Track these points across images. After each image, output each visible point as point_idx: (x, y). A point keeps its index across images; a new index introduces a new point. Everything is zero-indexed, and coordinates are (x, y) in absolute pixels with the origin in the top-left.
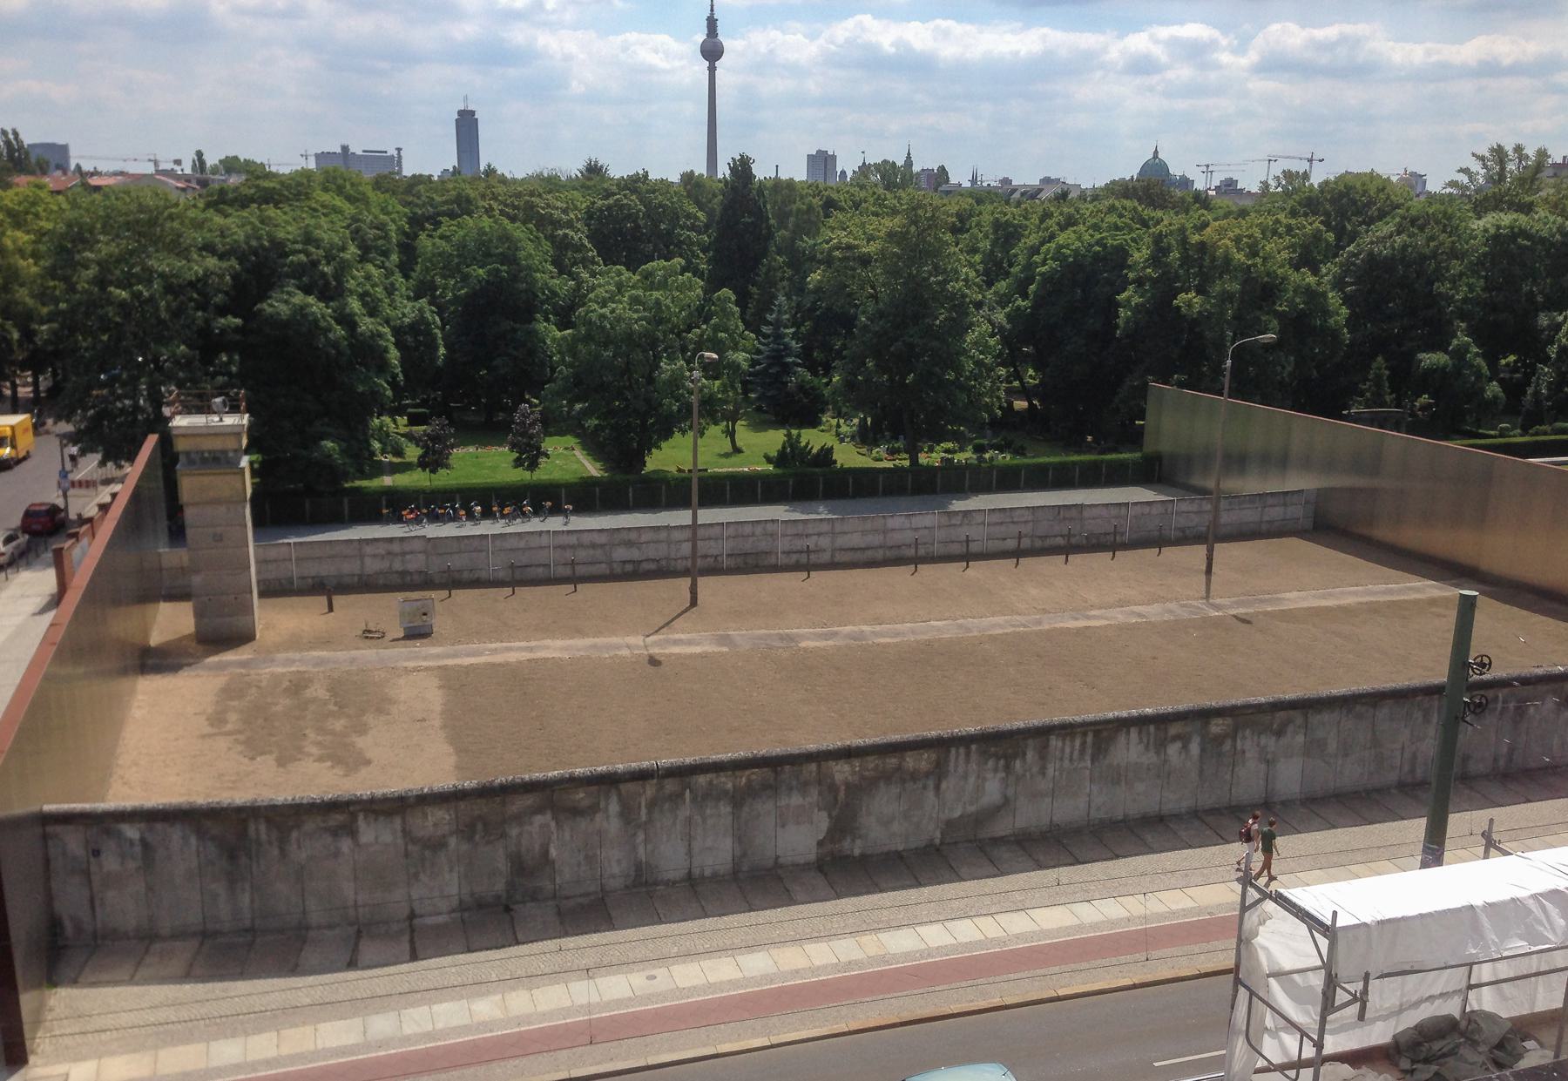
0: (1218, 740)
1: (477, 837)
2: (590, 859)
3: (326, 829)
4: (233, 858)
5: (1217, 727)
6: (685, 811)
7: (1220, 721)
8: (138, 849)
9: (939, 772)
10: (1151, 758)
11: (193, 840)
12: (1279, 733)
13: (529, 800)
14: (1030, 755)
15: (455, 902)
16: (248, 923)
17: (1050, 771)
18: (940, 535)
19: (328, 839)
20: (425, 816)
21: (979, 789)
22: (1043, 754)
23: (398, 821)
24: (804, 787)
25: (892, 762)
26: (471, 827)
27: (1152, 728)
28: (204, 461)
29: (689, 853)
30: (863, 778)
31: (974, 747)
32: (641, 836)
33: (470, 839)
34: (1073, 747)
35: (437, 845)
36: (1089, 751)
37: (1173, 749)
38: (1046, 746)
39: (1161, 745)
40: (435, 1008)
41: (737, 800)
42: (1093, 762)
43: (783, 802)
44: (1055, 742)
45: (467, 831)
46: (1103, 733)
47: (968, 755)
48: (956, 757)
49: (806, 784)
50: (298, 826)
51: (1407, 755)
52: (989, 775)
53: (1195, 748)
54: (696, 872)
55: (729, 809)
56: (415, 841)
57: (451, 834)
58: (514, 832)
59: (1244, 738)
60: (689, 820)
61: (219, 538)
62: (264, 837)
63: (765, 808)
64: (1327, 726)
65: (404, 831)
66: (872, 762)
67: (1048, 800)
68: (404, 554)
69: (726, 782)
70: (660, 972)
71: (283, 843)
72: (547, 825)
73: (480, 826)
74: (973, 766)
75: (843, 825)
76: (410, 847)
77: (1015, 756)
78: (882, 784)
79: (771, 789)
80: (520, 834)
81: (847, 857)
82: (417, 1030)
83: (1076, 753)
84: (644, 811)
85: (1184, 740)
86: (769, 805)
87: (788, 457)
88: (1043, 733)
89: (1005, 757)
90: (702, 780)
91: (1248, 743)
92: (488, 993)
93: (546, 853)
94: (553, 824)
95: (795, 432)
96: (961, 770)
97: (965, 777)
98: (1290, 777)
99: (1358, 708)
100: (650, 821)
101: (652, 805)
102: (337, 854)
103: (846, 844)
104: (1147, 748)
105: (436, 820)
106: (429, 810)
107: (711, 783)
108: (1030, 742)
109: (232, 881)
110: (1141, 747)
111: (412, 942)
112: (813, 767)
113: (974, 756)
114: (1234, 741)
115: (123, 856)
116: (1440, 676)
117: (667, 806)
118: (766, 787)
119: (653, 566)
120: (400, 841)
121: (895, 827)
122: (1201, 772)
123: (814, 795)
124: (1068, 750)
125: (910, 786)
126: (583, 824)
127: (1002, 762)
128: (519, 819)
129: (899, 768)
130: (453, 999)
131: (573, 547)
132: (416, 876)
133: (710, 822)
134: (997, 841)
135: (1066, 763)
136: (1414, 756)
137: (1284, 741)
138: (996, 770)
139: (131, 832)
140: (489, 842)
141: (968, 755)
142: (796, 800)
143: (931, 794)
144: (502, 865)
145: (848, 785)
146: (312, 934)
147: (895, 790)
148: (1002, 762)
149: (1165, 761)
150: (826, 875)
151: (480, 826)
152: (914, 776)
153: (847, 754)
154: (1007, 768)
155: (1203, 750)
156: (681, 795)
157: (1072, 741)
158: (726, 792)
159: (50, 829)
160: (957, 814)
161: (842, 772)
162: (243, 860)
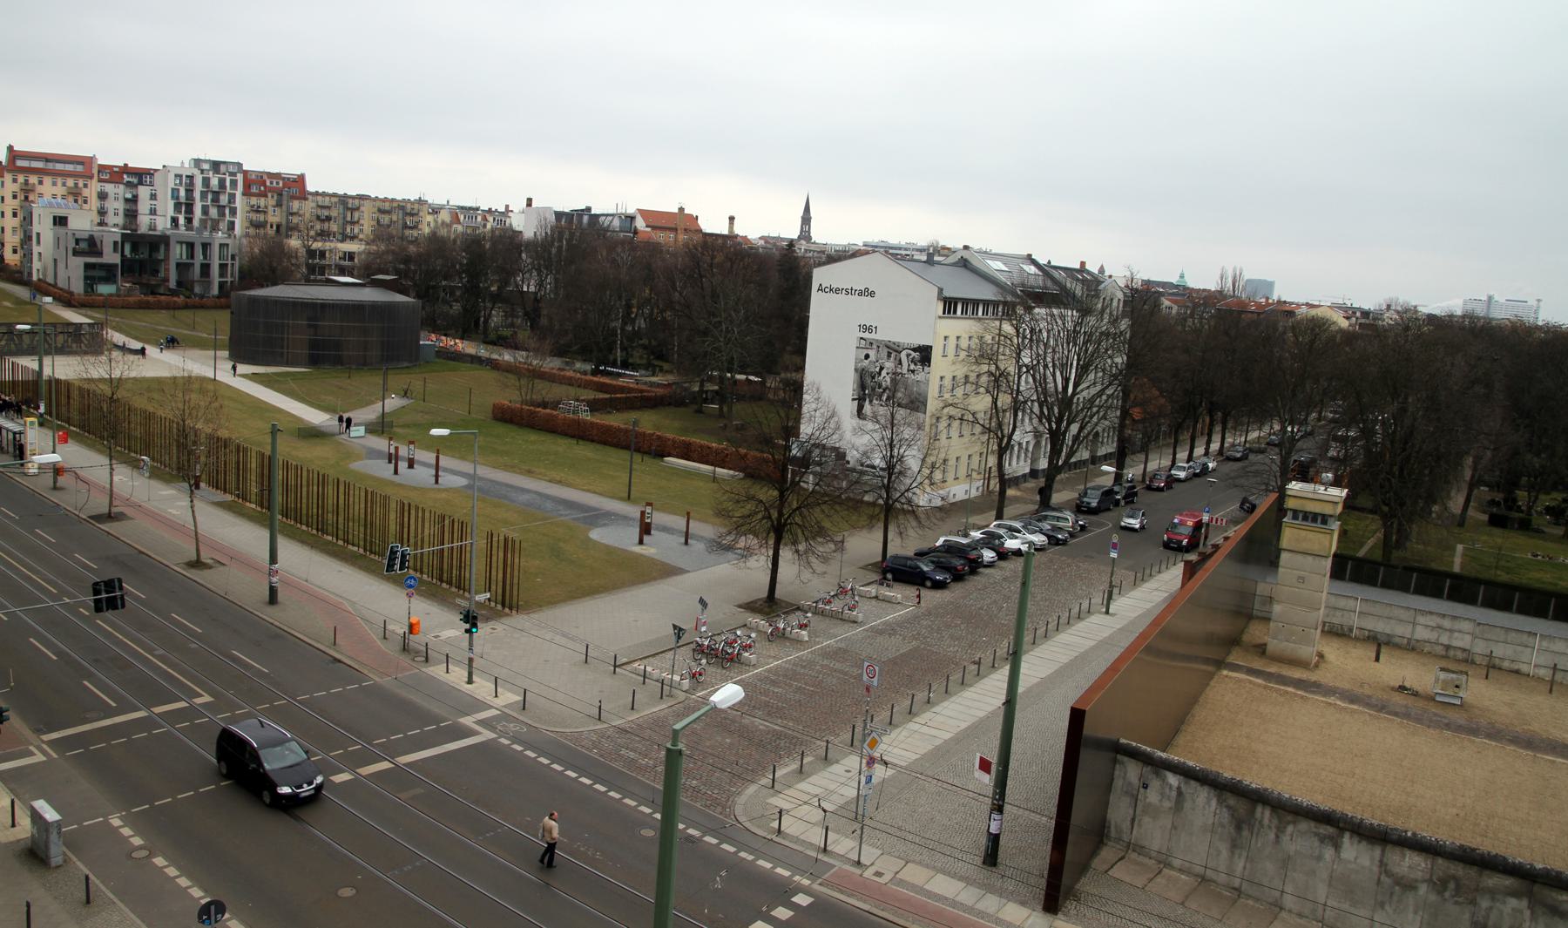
1: (1447, 894)
3: (1316, 834)
4: (1239, 828)
8: (1174, 794)
11: (1214, 803)
13: (1508, 882)
19: (1317, 843)
20: (1404, 856)
23: (1377, 851)
28: (1305, 518)
33: (1440, 893)
35: (1408, 886)
45: (1440, 885)
50: (1294, 823)
56: (1388, 874)
57: (1424, 881)
58: (1485, 903)
61: (1302, 579)
62: (1266, 822)
65: (1381, 861)
68: (1451, 631)
71: (1280, 830)
72: (1521, 912)
73: (1452, 885)
76: (1383, 878)
80: (1491, 908)
94: (1527, 913)
102: (1319, 858)
105: (1410, 864)
106: (1408, 853)
109: (1234, 846)
120: (1375, 869)
128: (1493, 893)
132: (1382, 905)
139: (1173, 780)
140: (1456, 903)
146: (1284, 914)
151: (1452, 885)
159: (1119, 757)
162: (1245, 833)
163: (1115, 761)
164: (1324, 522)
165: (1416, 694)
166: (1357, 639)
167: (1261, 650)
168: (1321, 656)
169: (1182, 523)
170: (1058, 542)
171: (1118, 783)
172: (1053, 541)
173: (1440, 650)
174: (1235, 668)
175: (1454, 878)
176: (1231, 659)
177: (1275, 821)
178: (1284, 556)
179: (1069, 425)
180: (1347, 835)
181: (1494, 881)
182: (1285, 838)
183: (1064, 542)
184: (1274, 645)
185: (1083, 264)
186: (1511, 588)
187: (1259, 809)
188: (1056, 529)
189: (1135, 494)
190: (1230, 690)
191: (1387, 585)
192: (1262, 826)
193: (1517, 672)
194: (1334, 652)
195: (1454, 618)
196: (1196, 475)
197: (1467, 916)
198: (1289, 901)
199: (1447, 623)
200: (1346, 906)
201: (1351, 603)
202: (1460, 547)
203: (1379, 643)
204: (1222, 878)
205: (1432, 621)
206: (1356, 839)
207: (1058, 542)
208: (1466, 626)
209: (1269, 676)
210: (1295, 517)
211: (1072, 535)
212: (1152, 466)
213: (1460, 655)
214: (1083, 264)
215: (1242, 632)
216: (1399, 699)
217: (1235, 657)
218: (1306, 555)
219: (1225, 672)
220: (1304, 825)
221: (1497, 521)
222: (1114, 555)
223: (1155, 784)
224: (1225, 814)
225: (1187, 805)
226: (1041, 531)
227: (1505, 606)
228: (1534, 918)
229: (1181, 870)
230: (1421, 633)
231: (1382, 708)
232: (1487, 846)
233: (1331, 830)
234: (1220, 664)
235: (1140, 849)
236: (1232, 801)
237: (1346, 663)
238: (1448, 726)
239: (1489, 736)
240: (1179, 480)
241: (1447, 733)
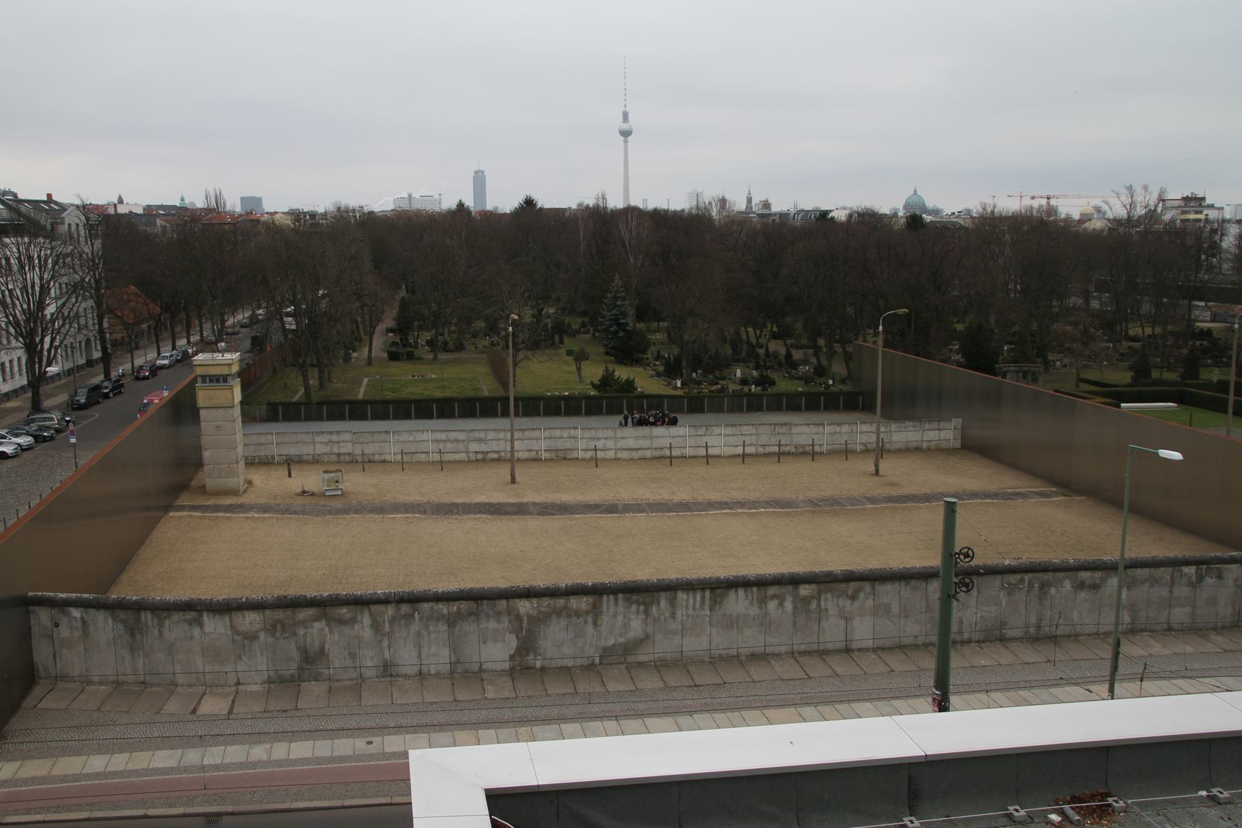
0: (807, 600)
1: (278, 634)
2: (352, 655)
4: (133, 635)
5: (804, 590)
6: (415, 627)
7: (807, 586)
8: (80, 624)
9: (595, 612)
10: (754, 611)
11: (110, 621)
12: (853, 598)
13: (310, 612)
14: (663, 603)
15: (265, 678)
16: (142, 678)
17: (679, 616)
18: (689, 442)
21: (626, 626)
22: (673, 603)
24: (499, 614)
25: (560, 602)
26: (274, 626)
27: (755, 589)
29: (419, 657)
30: (540, 612)
31: (620, 596)
32: (385, 643)
33: (273, 635)
35: (252, 637)
36: (708, 603)
37: (772, 605)
38: (675, 598)
39: (762, 602)
40: (229, 748)
41: (451, 621)
42: (711, 610)
43: (482, 626)
44: (681, 595)
45: (271, 629)
46: (719, 588)
47: (616, 600)
48: (607, 602)
49: (499, 614)
50: (169, 617)
52: (633, 617)
53: (788, 605)
54: (425, 669)
55: (445, 628)
58: (301, 632)
59: (826, 599)
60: (419, 634)
61: (218, 428)
62: (150, 623)
63: (469, 627)
64: (888, 592)
66: (546, 602)
67: (678, 637)
69: (443, 608)
70: (377, 740)
71: (161, 626)
73: (279, 627)
74: (621, 609)
75: (527, 646)
77: (651, 604)
78: (554, 617)
79: (476, 615)
81: (532, 668)
82: (212, 762)
83: (698, 604)
84: (387, 625)
86: (474, 627)
87: (606, 383)
88: (670, 588)
89: (644, 603)
90: (426, 606)
91: (829, 602)
92: (260, 742)
93: (322, 649)
94: (327, 629)
95: (611, 367)
97: (615, 616)
98: (864, 630)
99: (913, 582)
100: (390, 635)
101: (393, 621)
102: (192, 638)
103: (531, 657)
104: (752, 603)
105: (250, 620)
106: (246, 613)
107: (432, 608)
108: (662, 594)
109: (133, 649)
111: (233, 702)
112: (504, 602)
113: (621, 602)
114: (819, 600)
115: (71, 627)
116: (934, 560)
117: (403, 622)
118: (470, 614)
119: (495, 456)
120: (229, 633)
121: (565, 649)
122: (795, 622)
123: (505, 622)
124: (691, 601)
125: (574, 619)
126: (347, 630)
127: (642, 608)
128: (304, 623)
129: (565, 607)
130: (242, 743)
131: (444, 441)
132: (240, 657)
133: (433, 636)
134: (641, 665)
135: (691, 611)
137: (857, 604)
138: (638, 613)
139: (76, 613)
141: (616, 600)
142: (492, 624)
143: (590, 628)
144: (295, 655)
145: (530, 617)
146: (179, 689)
147: (564, 622)
148: (642, 608)
149: (766, 614)
150: (513, 680)
151: (279, 627)
152: (578, 614)
153: (529, 593)
154: (646, 612)
155: (795, 607)
156: (412, 615)
157: (694, 595)
158: (444, 616)
160: (610, 643)
162: (138, 637)
163: (28, 613)
164: (225, 381)
165: (313, 494)
166: (279, 463)
167: (203, 490)
168: (250, 483)
169: (151, 402)
170: (45, 440)
171: (35, 630)
172: (38, 439)
173: (334, 458)
174: (182, 508)
175: (279, 621)
176: (179, 502)
177: (156, 621)
178: (203, 413)
179: (43, 337)
180: (205, 614)
181: (304, 614)
182: (166, 631)
183: (51, 438)
184: (210, 483)
185: (49, 196)
186: (408, 402)
187: (143, 615)
188: (41, 429)
189: (122, 385)
190: (176, 526)
191: (308, 418)
192: (148, 627)
193: (384, 461)
194: (260, 478)
195: (338, 432)
196: (178, 361)
197: (293, 645)
198: (180, 679)
199: (334, 438)
200: (217, 668)
201: (269, 437)
202: (366, 380)
203: (290, 463)
204: (131, 678)
205: (324, 438)
206: (211, 615)
207: (45, 440)
208: (347, 437)
209: (216, 508)
210: (204, 382)
211: (58, 431)
212: (139, 362)
213: (347, 458)
214: (49, 196)
215: (191, 479)
216: (300, 501)
217: (184, 500)
218: (222, 412)
219: (171, 514)
220: (176, 616)
221: (394, 357)
222: (73, 440)
223: (64, 621)
224: (121, 627)
225: (91, 629)
226: (28, 434)
227: (385, 417)
228: (331, 632)
229: (100, 683)
230: (320, 449)
231: (287, 510)
232: (293, 591)
233: (193, 614)
234: (167, 508)
235: (65, 678)
236: (122, 615)
237: (268, 483)
238: (330, 512)
239: (357, 512)
240: (162, 367)
241: (329, 517)
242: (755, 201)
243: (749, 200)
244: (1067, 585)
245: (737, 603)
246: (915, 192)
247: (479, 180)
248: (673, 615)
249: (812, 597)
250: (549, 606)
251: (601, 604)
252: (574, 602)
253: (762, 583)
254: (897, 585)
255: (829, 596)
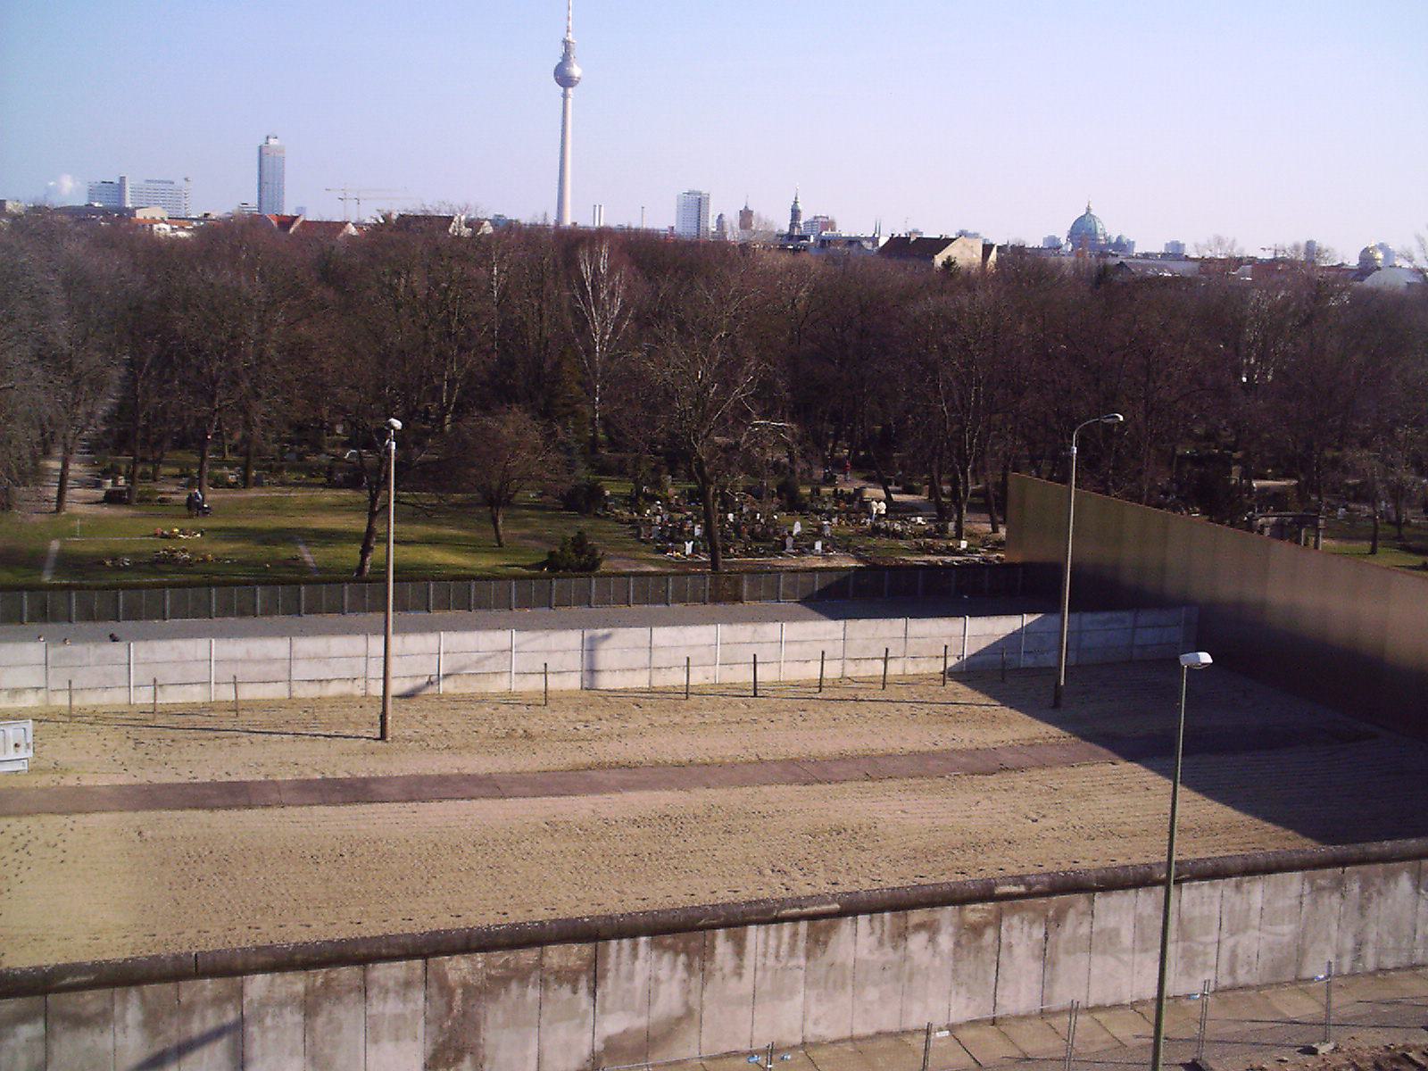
0: (977, 930)
5: (975, 913)
17: (748, 973)
25: (528, 956)
27: (887, 915)
30: (489, 977)
31: (643, 939)
34: (779, 939)
36: (802, 944)
37: (917, 942)
39: (901, 935)
42: (808, 957)
43: (377, 1007)
44: (754, 934)
51: (1225, 954)
53: (945, 941)
55: (298, 1018)
59: (1010, 927)
63: (348, 1015)
66: (500, 958)
78: (514, 986)
83: (784, 948)
85: (931, 928)
88: (736, 920)
96: (624, 969)
104: (881, 943)
110: (873, 939)
123: (418, 996)
124: (772, 943)
127: (682, 958)
133: (271, 1035)
135: (771, 962)
136: (1234, 955)
141: (635, 948)
145: (466, 986)
149: (905, 959)
155: (957, 944)
157: (779, 931)
161: (458, 968)
242: (805, 217)
243: (795, 213)
244: (1405, 883)
245: (857, 941)
246: (1088, 209)
247: (268, 167)
248: (738, 972)
249: (986, 924)
250: (506, 965)
251: (605, 957)
252: (555, 956)
253: (898, 904)
254: (1132, 892)
255: (1015, 920)
